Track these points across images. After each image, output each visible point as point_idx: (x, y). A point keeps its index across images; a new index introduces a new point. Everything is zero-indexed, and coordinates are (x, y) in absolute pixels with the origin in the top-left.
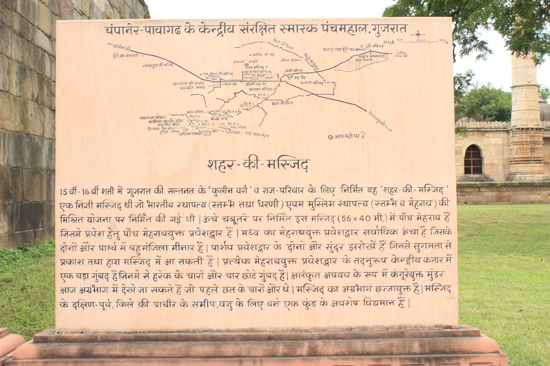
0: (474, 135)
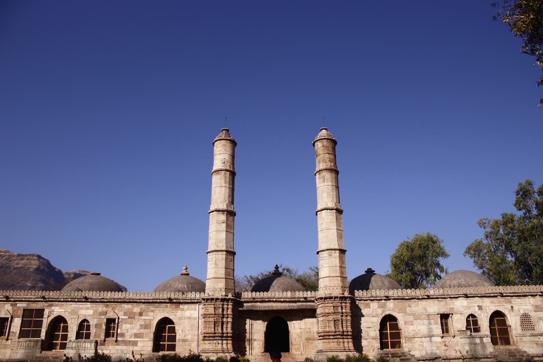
0: (167, 307)
